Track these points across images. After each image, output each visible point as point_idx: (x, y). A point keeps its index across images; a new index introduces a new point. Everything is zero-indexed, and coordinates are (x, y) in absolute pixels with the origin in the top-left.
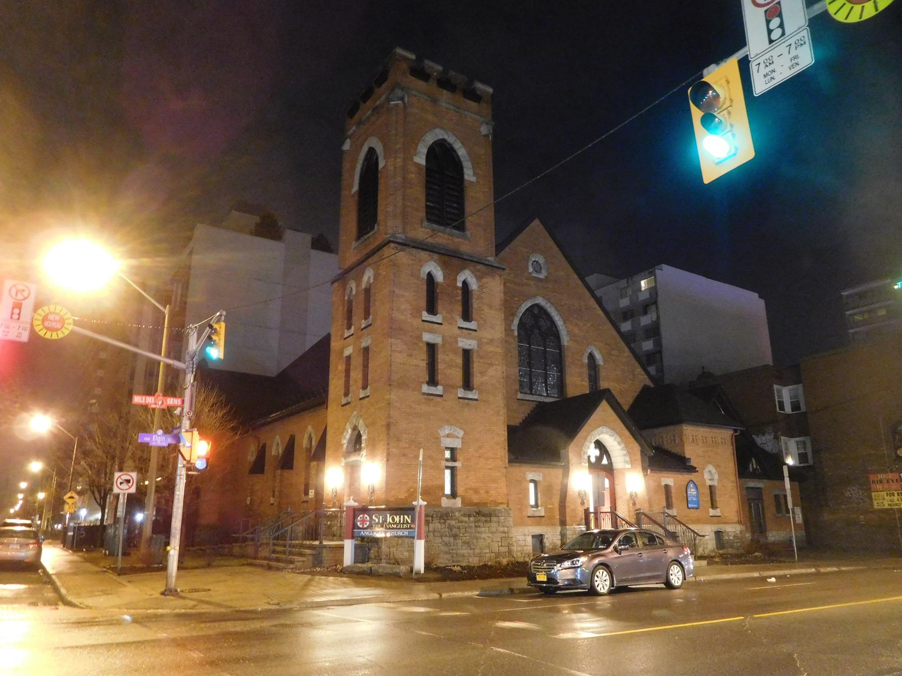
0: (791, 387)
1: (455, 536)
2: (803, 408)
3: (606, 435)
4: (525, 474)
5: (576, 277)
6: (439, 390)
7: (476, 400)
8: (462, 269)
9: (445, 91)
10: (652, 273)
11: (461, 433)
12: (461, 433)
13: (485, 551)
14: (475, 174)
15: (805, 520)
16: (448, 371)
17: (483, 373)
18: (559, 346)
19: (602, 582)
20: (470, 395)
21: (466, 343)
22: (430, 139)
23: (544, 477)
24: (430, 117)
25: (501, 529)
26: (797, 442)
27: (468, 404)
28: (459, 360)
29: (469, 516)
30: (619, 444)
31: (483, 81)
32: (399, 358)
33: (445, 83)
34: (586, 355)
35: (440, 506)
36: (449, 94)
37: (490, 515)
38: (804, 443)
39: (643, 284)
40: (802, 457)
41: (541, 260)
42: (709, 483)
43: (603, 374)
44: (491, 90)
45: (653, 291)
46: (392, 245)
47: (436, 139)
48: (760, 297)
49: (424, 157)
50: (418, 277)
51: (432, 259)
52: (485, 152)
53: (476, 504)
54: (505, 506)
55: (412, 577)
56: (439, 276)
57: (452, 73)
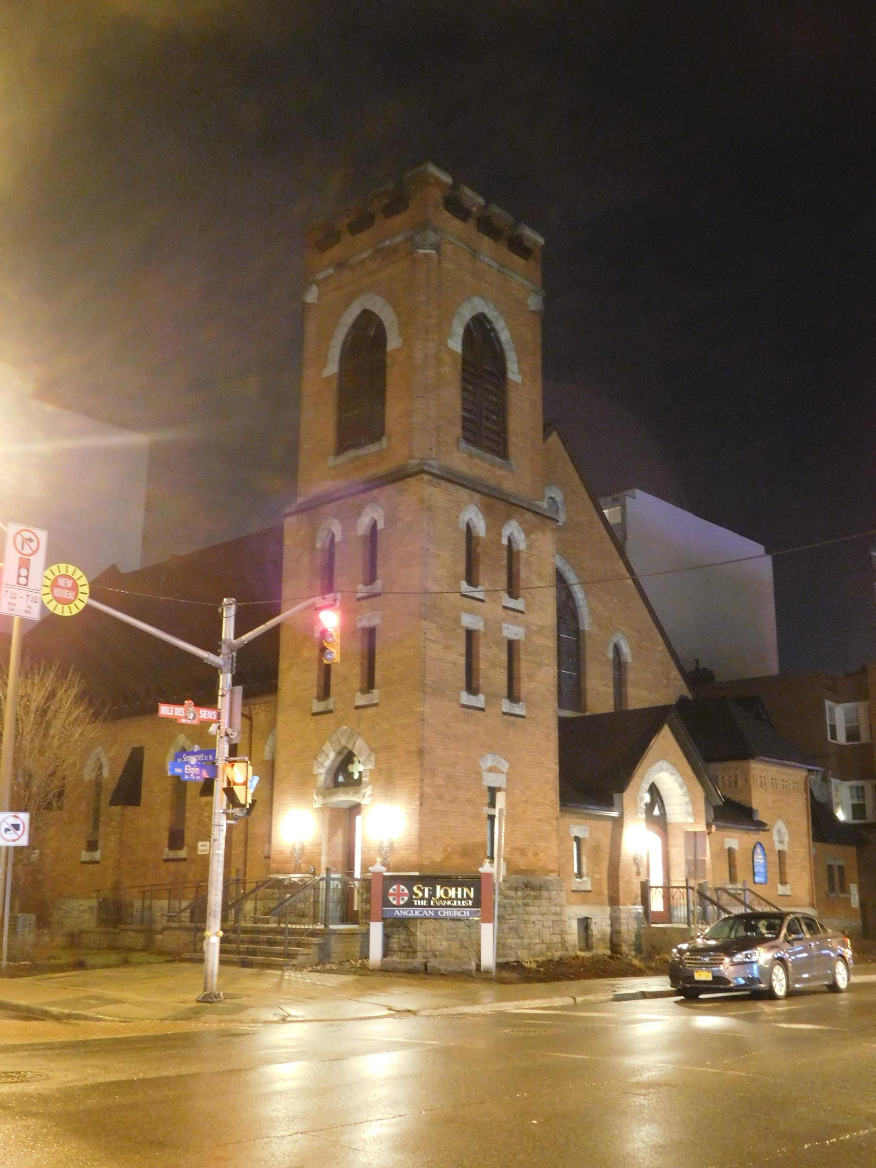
0: (847, 705)
2: (865, 737)
7: (523, 717)
8: (508, 517)
12: (505, 766)
13: (534, 941)
14: (521, 371)
15: (863, 904)
17: (531, 677)
20: (519, 709)
21: (512, 631)
22: (466, 313)
23: (591, 834)
25: (554, 909)
26: (851, 787)
30: (681, 786)
31: (534, 228)
32: (434, 650)
33: (487, 226)
34: (611, 646)
37: (540, 888)
38: (863, 788)
40: (858, 810)
42: (778, 847)
43: (631, 676)
44: (541, 241)
46: (426, 477)
47: (475, 313)
48: (768, 551)
49: (459, 340)
52: (533, 336)
53: (524, 872)
54: (555, 875)
55: (479, 975)
57: (495, 209)
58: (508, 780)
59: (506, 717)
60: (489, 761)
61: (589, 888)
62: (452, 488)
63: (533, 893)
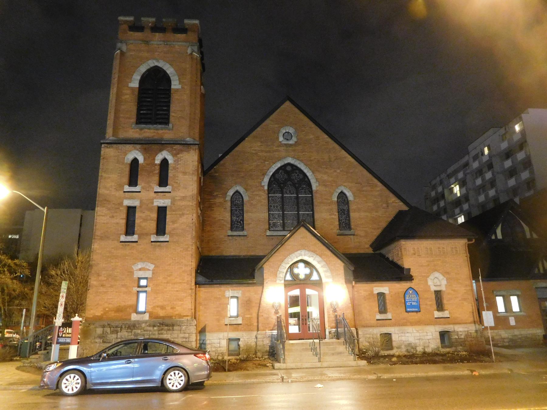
4: (224, 292)
6: (135, 238)
7: (168, 242)
8: (161, 150)
9: (157, 34)
10: (521, 119)
11: (152, 267)
12: (152, 267)
14: (180, 83)
16: (143, 224)
17: (174, 222)
18: (311, 192)
19: (175, 381)
24: (146, 54)
25: (182, 335)
27: (159, 246)
28: (154, 215)
29: (154, 326)
31: (189, 18)
33: (156, 29)
35: (130, 319)
36: (161, 34)
37: (173, 325)
39: (517, 128)
41: (291, 130)
42: (433, 289)
44: (197, 22)
45: (523, 132)
47: (149, 67)
50: (123, 163)
51: (136, 149)
53: (163, 318)
56: (141, 159)
58: (153, 273)
59: (153, 243)
60: (140, 265)
61: (241, 323)
62: (120, 146)
63: (166, 328)
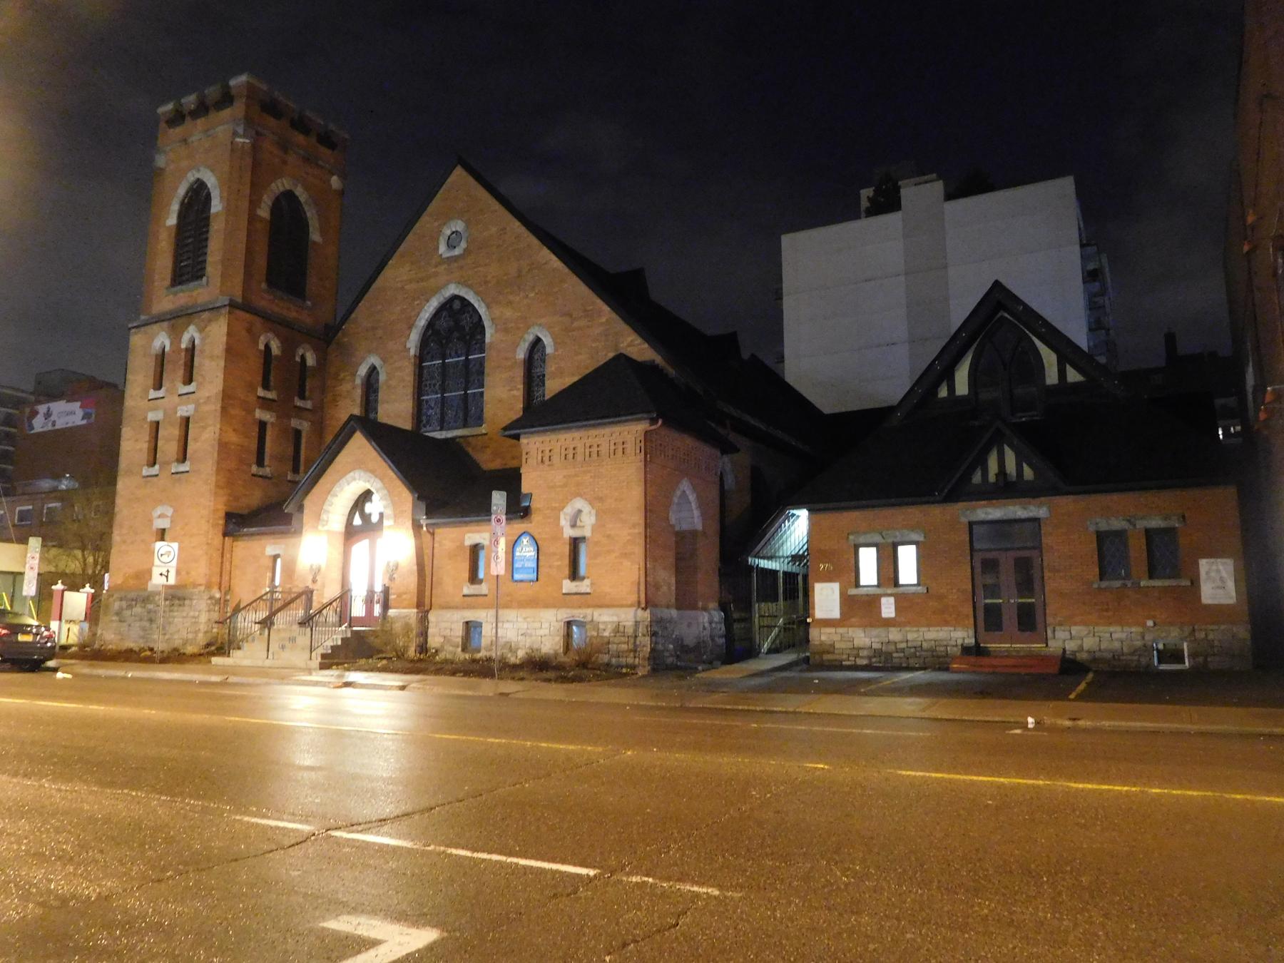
1: (151, 621)
3: (358, 481)
5: (518, 223)
12: (169, 511)
35: (146, 589)
